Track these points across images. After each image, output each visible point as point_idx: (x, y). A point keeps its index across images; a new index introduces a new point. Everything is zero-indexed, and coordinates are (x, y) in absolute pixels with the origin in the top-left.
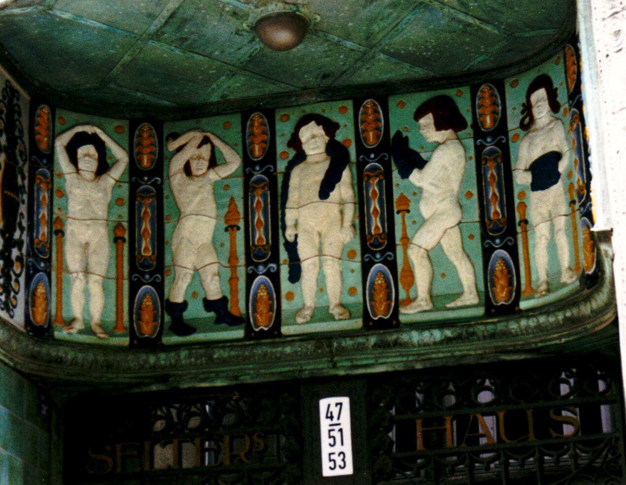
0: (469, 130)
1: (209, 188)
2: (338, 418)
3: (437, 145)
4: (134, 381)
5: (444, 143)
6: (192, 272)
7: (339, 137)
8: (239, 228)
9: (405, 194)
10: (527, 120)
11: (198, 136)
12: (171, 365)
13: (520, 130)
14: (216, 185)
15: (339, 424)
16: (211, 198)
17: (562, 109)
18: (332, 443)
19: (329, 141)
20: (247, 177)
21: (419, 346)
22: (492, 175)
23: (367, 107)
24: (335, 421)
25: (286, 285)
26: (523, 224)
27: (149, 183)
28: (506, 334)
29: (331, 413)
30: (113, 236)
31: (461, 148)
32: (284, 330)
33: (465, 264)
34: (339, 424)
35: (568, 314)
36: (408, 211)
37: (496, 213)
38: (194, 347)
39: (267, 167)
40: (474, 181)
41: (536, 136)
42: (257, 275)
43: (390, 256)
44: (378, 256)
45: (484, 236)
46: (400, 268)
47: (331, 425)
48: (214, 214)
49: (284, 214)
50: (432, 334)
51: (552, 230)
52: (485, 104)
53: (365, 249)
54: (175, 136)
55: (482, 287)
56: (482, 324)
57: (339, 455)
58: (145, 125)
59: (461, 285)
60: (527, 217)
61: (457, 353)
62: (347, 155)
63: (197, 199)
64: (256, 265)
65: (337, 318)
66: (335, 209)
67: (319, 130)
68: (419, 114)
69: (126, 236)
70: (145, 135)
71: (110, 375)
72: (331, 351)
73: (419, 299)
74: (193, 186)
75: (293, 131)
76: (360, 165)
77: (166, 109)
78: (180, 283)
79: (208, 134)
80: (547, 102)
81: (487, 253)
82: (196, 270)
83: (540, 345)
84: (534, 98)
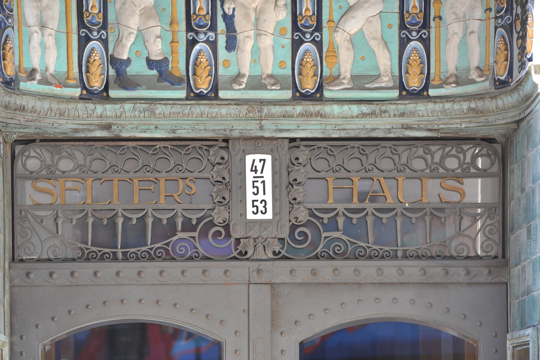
2: (262, 172)
4: (81, 127)
6: (136, 32)
12: (116, 116)
15: (263, 177)
18: (256, 192)
24: (259, 174)
26: (437, 20)
28: (412, 114)
29: (256, 167)
32: (222, 94)
33: (383, 50)
34: (263, 177)
35: (473, 105)
37: (414, 7)
38: (139, 102)
42: (198, 42)
43: (318, 36)
44: (308, 36)
45: (402, 26)
46: (325, 49)
47: (254, 177)
50: (350, 109)
51: (467, 33)
53: (295, 27)
55: (397, 73)
56: (394, 104)
57: (261, 203)
59: (378, 68)
60: (441, 15)
61: (369, 126)
64: (197, 33)
65: (269, 87)
71: (61, 122)
72: (261, 116)
73: (342, 77)
78: (124, 41)
81: (403, 43)
82: (139, 31)
83: (441, 126)
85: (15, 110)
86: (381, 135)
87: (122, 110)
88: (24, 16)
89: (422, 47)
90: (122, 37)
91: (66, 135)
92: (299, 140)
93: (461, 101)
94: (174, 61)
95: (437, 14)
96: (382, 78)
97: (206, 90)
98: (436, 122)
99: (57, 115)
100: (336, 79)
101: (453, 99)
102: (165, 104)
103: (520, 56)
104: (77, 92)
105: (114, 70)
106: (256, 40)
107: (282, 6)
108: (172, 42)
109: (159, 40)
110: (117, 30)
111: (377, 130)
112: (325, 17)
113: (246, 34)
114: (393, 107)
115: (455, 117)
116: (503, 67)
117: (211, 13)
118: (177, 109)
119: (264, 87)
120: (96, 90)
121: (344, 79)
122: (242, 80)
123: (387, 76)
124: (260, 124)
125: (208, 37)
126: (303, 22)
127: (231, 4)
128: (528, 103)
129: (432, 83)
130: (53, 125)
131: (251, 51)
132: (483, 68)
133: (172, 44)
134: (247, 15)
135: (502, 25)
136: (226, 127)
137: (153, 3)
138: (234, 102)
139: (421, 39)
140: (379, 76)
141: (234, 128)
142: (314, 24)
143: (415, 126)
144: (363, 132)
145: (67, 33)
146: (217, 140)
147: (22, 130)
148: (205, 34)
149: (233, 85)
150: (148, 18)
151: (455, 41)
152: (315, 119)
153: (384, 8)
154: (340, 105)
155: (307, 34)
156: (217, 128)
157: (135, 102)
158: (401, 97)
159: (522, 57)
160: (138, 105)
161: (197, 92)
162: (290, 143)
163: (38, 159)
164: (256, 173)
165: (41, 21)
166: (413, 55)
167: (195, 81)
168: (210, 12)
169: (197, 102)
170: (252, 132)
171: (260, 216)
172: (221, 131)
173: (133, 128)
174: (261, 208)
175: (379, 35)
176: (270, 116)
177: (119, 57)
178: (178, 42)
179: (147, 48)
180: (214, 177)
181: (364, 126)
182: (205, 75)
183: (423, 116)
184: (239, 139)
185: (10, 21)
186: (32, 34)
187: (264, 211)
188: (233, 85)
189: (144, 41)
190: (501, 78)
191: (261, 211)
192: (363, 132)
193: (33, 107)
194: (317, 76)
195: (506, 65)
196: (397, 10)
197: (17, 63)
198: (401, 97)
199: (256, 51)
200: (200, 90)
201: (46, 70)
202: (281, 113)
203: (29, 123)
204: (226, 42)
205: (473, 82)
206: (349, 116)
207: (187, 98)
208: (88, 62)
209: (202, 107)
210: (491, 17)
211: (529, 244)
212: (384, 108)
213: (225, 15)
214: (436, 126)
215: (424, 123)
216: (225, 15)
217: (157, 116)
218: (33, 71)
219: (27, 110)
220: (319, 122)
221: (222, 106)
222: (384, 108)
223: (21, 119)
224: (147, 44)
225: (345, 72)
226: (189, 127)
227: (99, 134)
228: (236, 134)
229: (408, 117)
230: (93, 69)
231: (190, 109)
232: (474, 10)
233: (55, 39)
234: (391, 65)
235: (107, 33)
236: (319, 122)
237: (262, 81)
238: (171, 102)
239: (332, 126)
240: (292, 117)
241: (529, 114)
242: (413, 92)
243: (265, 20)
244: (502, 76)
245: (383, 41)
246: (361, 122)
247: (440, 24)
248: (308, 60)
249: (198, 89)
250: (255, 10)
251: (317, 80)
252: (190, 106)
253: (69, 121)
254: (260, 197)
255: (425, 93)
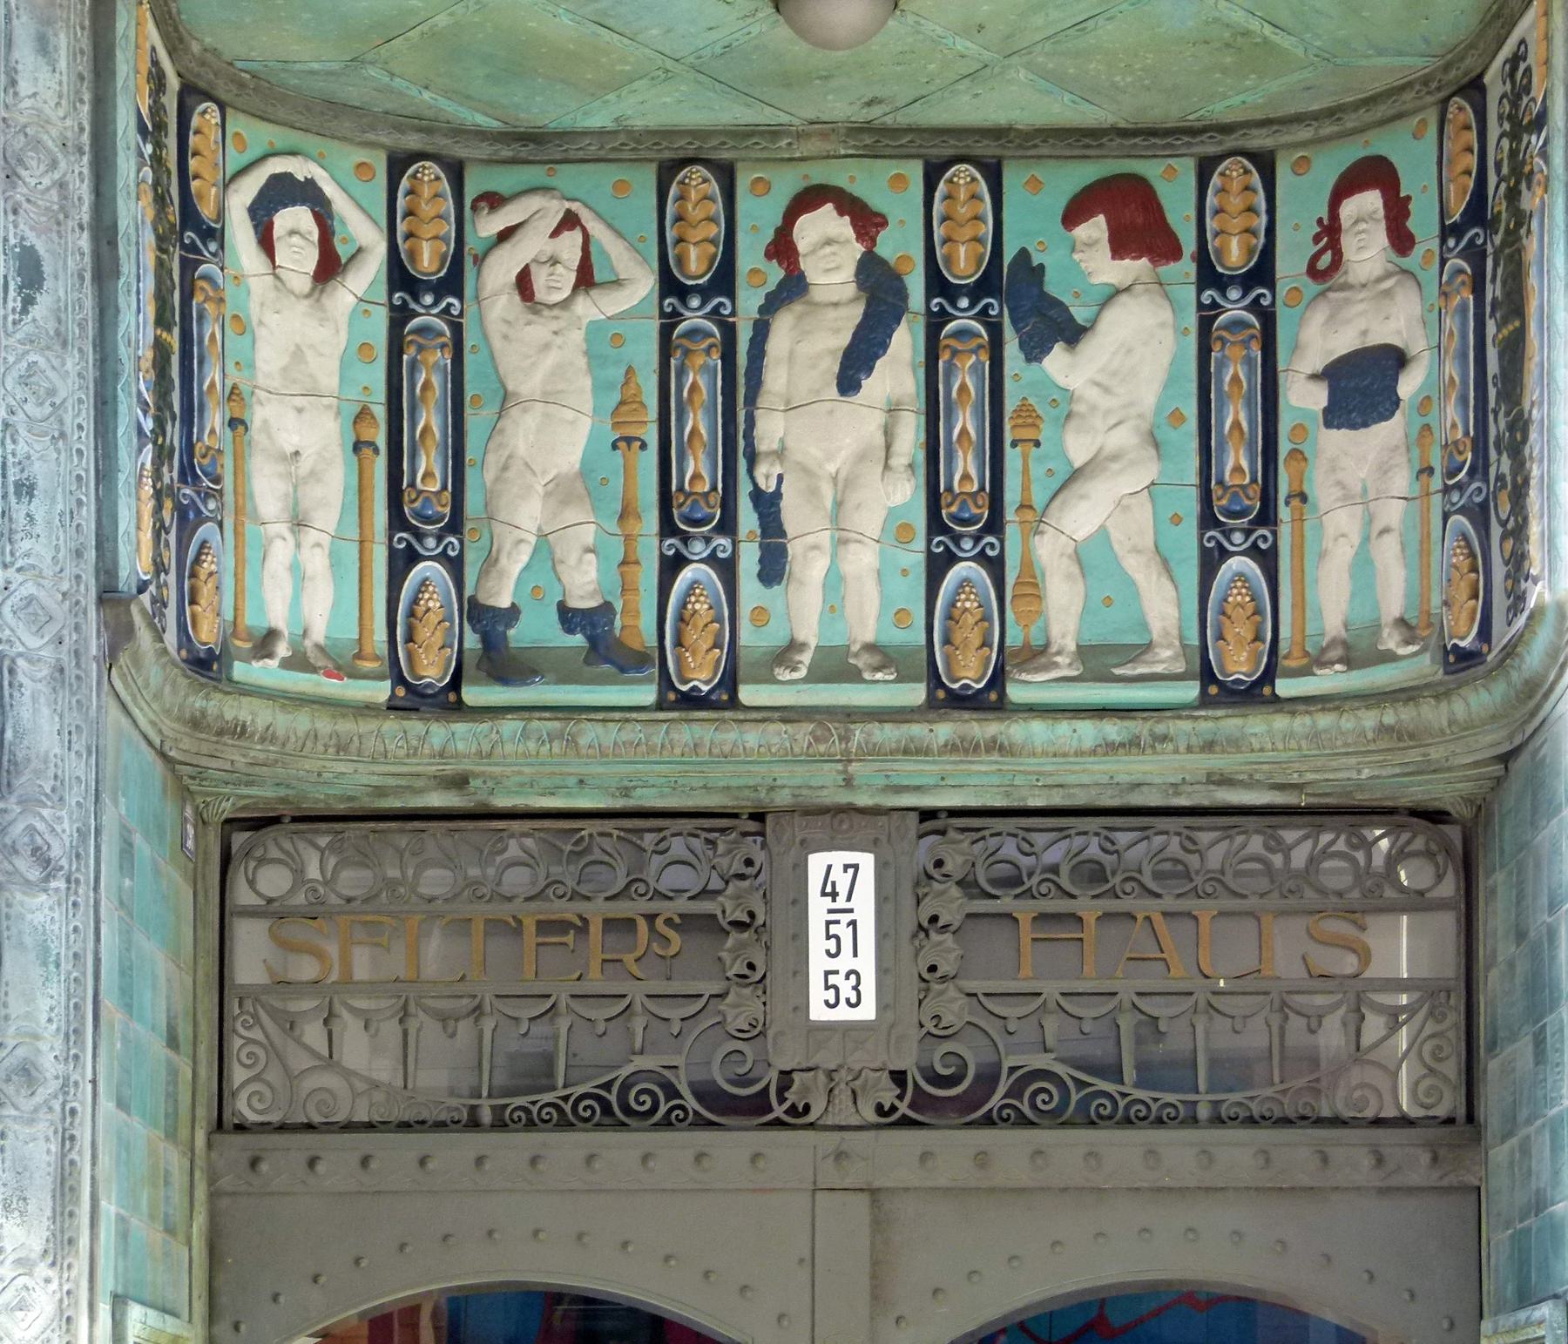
0: (1186, 268)
1: (577, 337)
2: (849, 899)
3: (1114, 293)
4: (391, 782)
5: (1127, 289)
6: (533, 539)
7: (887, 246)
8: (644, 446)
9: (1031, 401)
10: (1326, 259)
11: (555, 210)
13: (1307, 280)
14: (594, 329)
15: (851, 911)
16: (582, 362)
17: (1418, 251)
18: (833, 951)
19: (864, 255)
20: (669, 322)
21: (1045, 754)
22: (1235, 379)
23: (957, 184)
24: (841, 903)
25: (749, 587)
26: (1296, 502)
27: (435, 311)
28: (1235, 744)
29: (834, 884)
30: (351, 439)
31: (1166, 304)
33: (1158, 578)
34: (851, 911)
35: (1389, 718)
36: (1037, 444)
37: (1238, 469)
38: (537, 715)
39: (716, 301)
40: (1192, 387)
41: (1347, 301)
42: (688, 562)
43: (992, 546)
44: (967, 544)
45: (1208, 519)
46: (1011, 577)
47: (831, 911)
48: (588, 406)
49: (751, 422)
50: (1075, 731)
51: (1371, 533)
52: (1228, 208)
53: (935, 524)
54: (494, 201)
57: (847, 977)
58: (424, 167)
60: (1306, 488)
61: (1123, 778)
62: (901, 294)
63: (551, 359)
64: (686, 539)
66: (872, 424)
67: (843, 227)
68: (1074, 214)
69: (381, 441)
70: (426, 192)
71: (341, 767)
72: (847, 752)
74: (539, 330)
75: (779, 222)
76: (935, 323)
77: (482, 135)
78: (503, 561)
79: (575, 206)
80: (1383, 225)
81: (1210, 561)
82: (542, 536)
83: (1310, 777)
84: (1350, 208)
85: (220, 733)
86: (1154, 800)
87: (494, 736)
88: (252, 497)
89: (1258, 572)
90: (499, 551)
91: (356, 805)
92: (943, 815)
93: (1358, 709)
94: (631, 611)
95: (1296, 488)
96: (1157, 650)
97: (707, 683)
98: (1297, 765)
99: (331, 750)
100: (1036, 655)
101: (1337, 703)
102: (603, 721)
103: (1510, 582)
104: (381, 691)
105: (477, 636)
106: (834, 556)
107: (902, 469)
108: (624, 563)
109: (591, 556)
110: (486, 536)
111: (1145, 789)
112: (1011, 496)
113: (810, 539)
114: (1186, 725)
115: (1343, 750)
116: (1464, 615)
117: (723, 489)
118: (633, 733)
119: (854, 676)
120: (429, 685)
121: (1059, 653)
122: (798, 658)
123: (1169, 646)
124: (845, 771)
125: (714, 550)
126: (954, 509)
127: (772, 465)
128: (1532, 704)
129: (1285, 663)
130: (319, 775)
131: (824, 585)
132: (1414, 622)
133: (625, 568)
134: (813, 493)
135: (1463, 506)
136: (759, 780)
137: (578, 466)
138: (777, 715)
139: (1254, 552)
140: (1148, 647)
141: (779, 782)
142: (982, 514)
143: (1241, 777)
144: (1109, 792)
145: (361, 542)
146: (735, 816)
147: (245, 791)
148: (708, 540)
149: (777, 671)
150: (565, 502)
151: (1342, 554)
152: (985, 758)
153: (1161, 473)
154: (1050, 722)
155: (966, 539)
156: (734, 783)
157: (526, 715)
158: (1205, 701)
159: (1516, 581)
160: (535, 724)
161: (684, 688)
162: (921, 821)
163: (287, 865)
164: (834, 900)
165: (294, 510)
166: (1235, 591)
167: (679, 661)
168: (720, 486)
169: (683, 715)
170: (825, 792)
171: (843, 1013)
172: (747, 793)
173: (522, 785)
174: (847, 991)
175: (1151, 545)
176: (873, 752)
177: (491, 602)
178: (637, 563)
179: (559, 580)
180: (728, 912)
181: (1112, 777)
182: (705, 647)
183: (1262, 750)
184: (790, 811)
185: (212, 505)
186: (270, 541)
187: (853, 1000)
188: (777, 671)
189: (553, 560)
190: (1462, 644)
191: (848, 1001)
192: (1109, 792)
193: (268, 728)
194: (991, 647)
195: (1474, 611)
196: (1194, 479)
197: (229, 615)
198: (1205, 701)
199: (834, 582)
200: (691, 684)
201: (305, 633)
202: (898, 741)
203: (257, 770)
204: (760, 561)
205: (1389, 657)
206: (1072, 751)
207: (660, 705)
208: (411, 614)
209: (696, 727)
210: (1432, 489)
211: (1541, 1077)
212: (1160, 728)
213: (757, 495)
214: (1295, 775)
215: (1265, 767)
216: (757, 495)
217: (584, 751)
218: (272, 635)
219: (252, 735)
220: (995, 767)
221: (747, 726)
222: (1160, 728)
223: (236, 758)
224: (560, 568)
225: (1063, 637)
226: (663, 780)
227: (437, 800)
228: (783, 798)
229: (1223, 752)
230: (423, 632)
231: (667, 732)
232: (1390, 474)
233: (331, 555)
234: (1180, 619)
235: (461, 543)
236: (995, 767)
237: (852, 661)
238: (617, 715)
239: (1029, 777)
240: (926, 754)
241: (1536, 731)
242: (1235, 687)
243: (859, 505)
244: (1462, 638)
245: (1158, 558)
246: (1101, 767)
247: (1302, 514)
248: (968, 605)
249: (685, 682)
250: (835, 479)
251: (988, 659)
252: (665, 726)
253: (360, 766)
254: (845, 962)
255: (1267, 690)
